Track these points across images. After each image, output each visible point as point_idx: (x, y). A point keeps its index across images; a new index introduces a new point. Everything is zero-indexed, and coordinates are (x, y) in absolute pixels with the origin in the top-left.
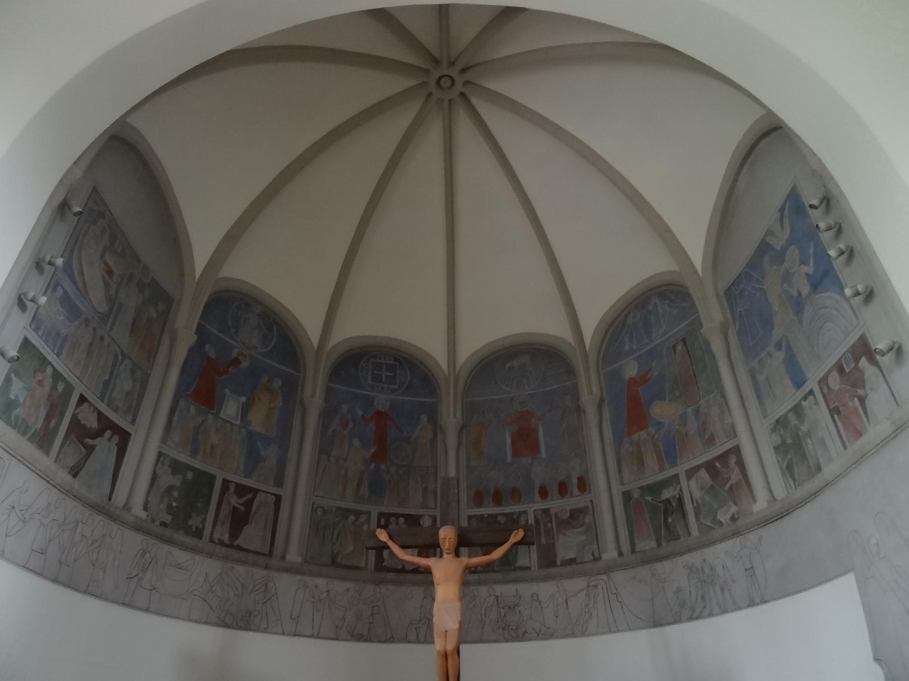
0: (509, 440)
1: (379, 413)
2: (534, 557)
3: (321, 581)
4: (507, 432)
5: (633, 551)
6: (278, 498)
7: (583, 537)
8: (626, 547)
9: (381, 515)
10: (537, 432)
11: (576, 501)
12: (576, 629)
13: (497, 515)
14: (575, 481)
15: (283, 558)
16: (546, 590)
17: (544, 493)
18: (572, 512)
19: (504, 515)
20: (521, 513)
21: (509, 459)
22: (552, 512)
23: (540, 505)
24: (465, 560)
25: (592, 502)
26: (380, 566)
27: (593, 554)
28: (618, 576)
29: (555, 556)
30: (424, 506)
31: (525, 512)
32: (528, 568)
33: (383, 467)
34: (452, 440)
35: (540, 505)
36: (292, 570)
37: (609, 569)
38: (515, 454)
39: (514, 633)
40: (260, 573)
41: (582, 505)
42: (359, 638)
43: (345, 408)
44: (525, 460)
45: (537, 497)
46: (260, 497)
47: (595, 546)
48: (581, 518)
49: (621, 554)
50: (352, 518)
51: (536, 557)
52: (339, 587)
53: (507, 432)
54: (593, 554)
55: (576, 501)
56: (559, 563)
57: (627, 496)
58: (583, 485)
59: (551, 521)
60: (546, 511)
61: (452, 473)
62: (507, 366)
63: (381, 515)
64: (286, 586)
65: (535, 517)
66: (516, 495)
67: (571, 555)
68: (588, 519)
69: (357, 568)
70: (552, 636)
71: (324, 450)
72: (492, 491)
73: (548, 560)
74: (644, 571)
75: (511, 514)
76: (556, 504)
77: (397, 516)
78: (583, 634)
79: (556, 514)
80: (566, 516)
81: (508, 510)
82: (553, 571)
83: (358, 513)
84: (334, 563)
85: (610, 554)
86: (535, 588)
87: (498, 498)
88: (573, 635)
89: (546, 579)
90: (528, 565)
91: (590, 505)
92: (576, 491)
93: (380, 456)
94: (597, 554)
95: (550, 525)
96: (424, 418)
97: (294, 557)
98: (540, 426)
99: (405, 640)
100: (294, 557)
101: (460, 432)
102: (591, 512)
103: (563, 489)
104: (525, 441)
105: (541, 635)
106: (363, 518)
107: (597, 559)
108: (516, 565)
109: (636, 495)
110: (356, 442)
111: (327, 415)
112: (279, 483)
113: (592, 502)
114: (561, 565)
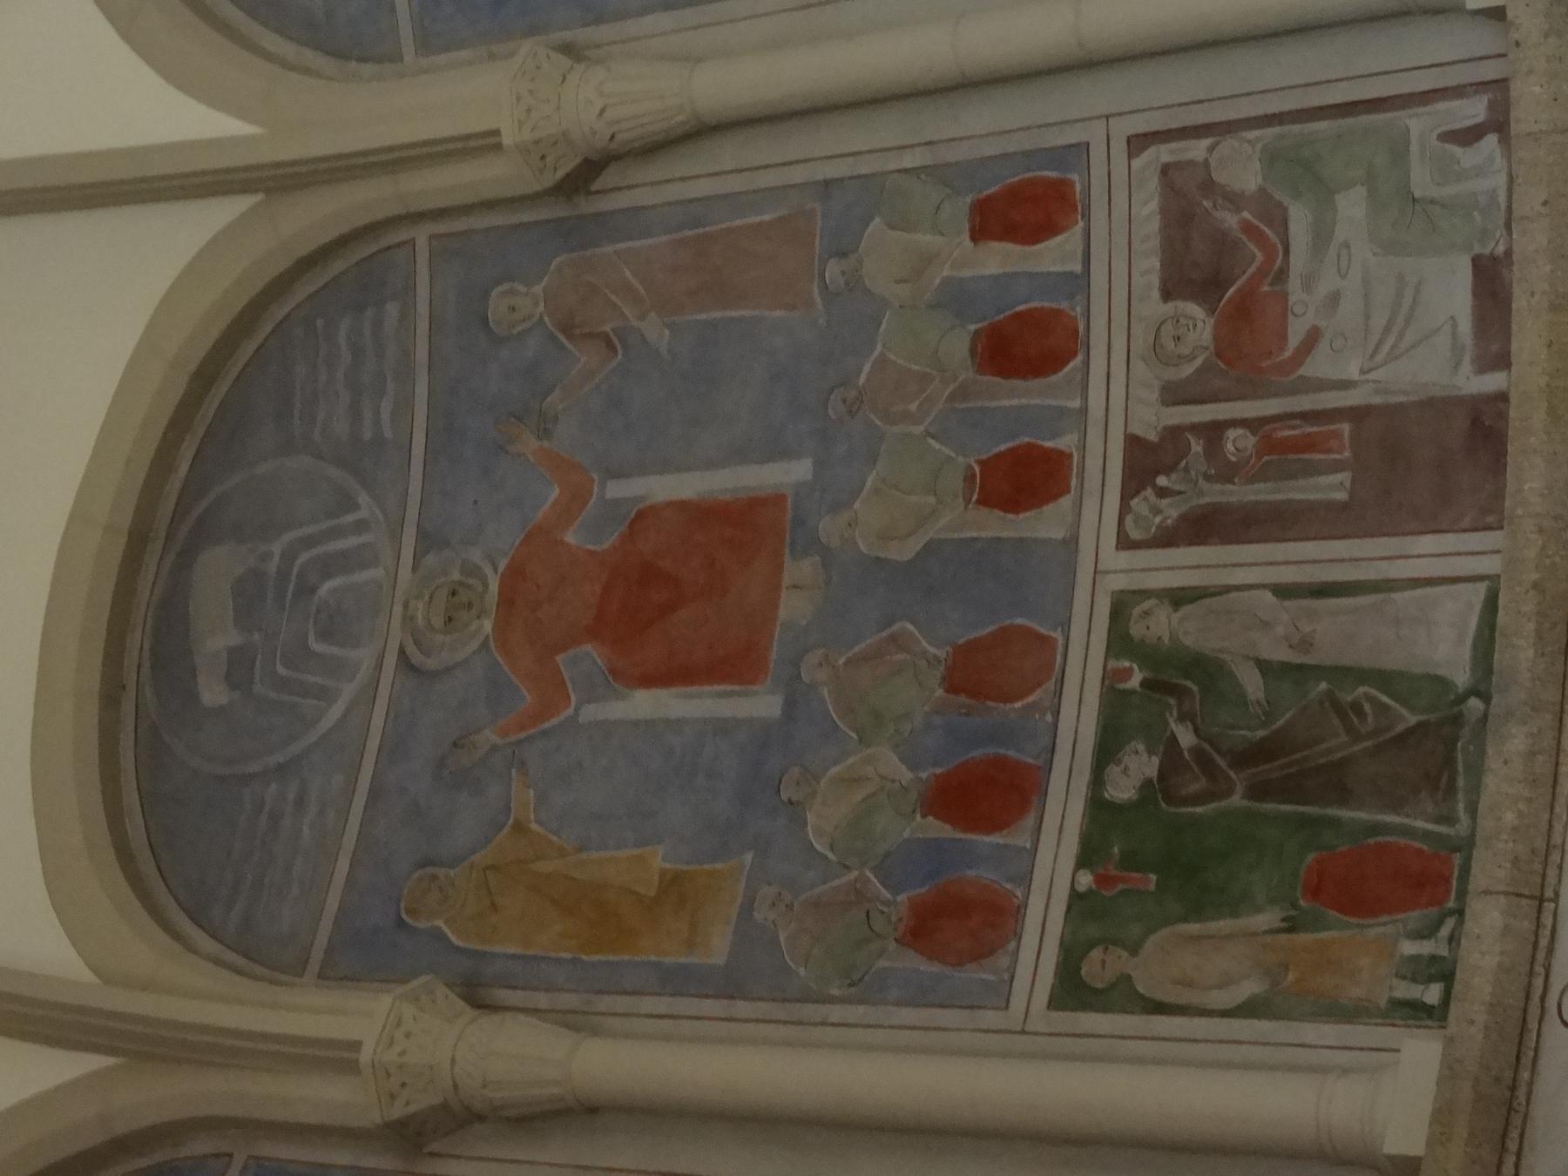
0: (644, 703)
2: (1427, 552)
4: (593, 712)
7: (1352, 207)
10: (644, 517)
11: (1114, 259)
13: (1098, 805)
14: (998, 258)
19: (1106, 752)
20: (1120, 642)
22: (1151, 419)
25: (1138, 143)
27: (1468, 136)
29: (1437, 406)
31: (1120, 607)
38: (735, 665)
41: (1149, 208)
44: (793, 608)
45: (1045, 523)
47: (1419, 124)
48: (1230, 220)
51: (1428, 543)
53: (593, 712)
54: (1468, 136)
55: (1114, 259)
56: (1493, 382)
58: (1026, 206)
59: (1213, 432)
62: (213, 693)
65: (1167, 539)
66: (996, 668)
67: (1451, 295)
68: (1242, 168)
72: (937, 829)
75: (1114, 700)
76: (1112, 396)
79: (1174, 395)
80: (1199, 325)
87: (986, 793)
90: (1482, 587)
91: (1165, 153)
92: (1054, 255)
94: (1474, 110)
95: (1237, 442)
98: (617, 490)
102: (1197, 149)
103: (1026, 345)
104: (671, 596)
108: (1462, 679)
113: (1138, 143)
114: (1502, 361)
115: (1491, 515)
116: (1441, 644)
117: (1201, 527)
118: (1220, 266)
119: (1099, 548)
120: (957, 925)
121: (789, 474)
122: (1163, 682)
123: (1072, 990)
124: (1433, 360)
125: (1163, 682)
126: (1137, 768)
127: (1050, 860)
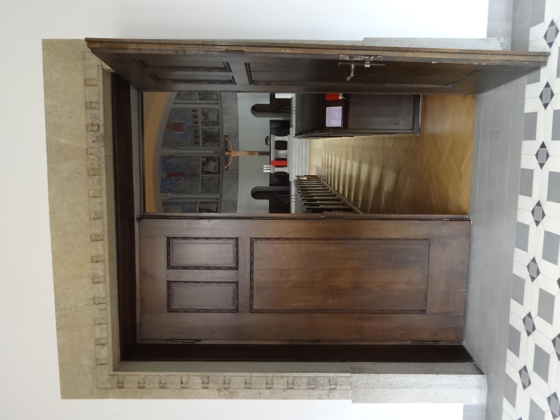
0: (177, 132)
1: (168, 175)
2: (216, 127)
3: (224, 188)
5: (217, 100)
6: (200, 203)
8: (216, 102)
9: (202, 173)
12: (236, 118)
14: (193, 113)
15: (218, 199)
16: (226, 125)
17: (196, 123)
18: (203, 115)
21: (184, 133)
23: (200, 124)
24: (232, 150)
26: (218, 173)
28: (223, 106)
30: (199, 160)
32: (219, 130)
33: (187, 173)
34: (177, 151)
35: (200, 124)
36: (221, 196)
37: (221, 108)
38: (182, 130)
39: (236, 135)
40: (223, 204)
42: (238, 177)
43: (167, 187)
44: (185, 128)
45: (197, 125)
46: (201, 207)
49: (217, 104)
50: (204, 182)
52: (224, 183)
55: (200, 114)
57: (200, 99)
58: (195, 111)
60: (202, 122)
61: (212, 152)
63: (202, 173)
64: (225, 197)
66: (196, 131)
67: (216, 117)
68: (205, 110)
69: (219, 180)
70: (238, 125)
71: (184, 192)
73: (217, 123)
74: (223, 99)
76: (200, 119)
77: (203, 168)
78: (237, 116)
80: (204, 117)
81: (201, 134)
82: (220, 123)
83: (203, 180)
84: (218, 186)
85: (217, 107)
86: (225, 128)
87: (197, 137)
88: (238, 120)
89: (222, 124)
92: (196, 113)
93: (183, 175)
96: (168, 160)
97: (218, 196)
99: (238, 165)
100: (218, 196)
101: (175, 149)
103: (195, 117)
105: (237, 128)
106: (204, 179)
107: (218, 110)
109: (201, 97)
110: (179, 182)
111: (171, 192)
112: (197, 203)
115: (219, 125)
116: (217, 131)
117: (205, 125)
118: (204, 114)
119: (201, 127)
120: (197, 143)
121: (183, 122)
122: (204, 132)
123: (203, 146)
124: (215, 119)
125: (204, 132)
126: (204, 136)
127: (201, 141)
